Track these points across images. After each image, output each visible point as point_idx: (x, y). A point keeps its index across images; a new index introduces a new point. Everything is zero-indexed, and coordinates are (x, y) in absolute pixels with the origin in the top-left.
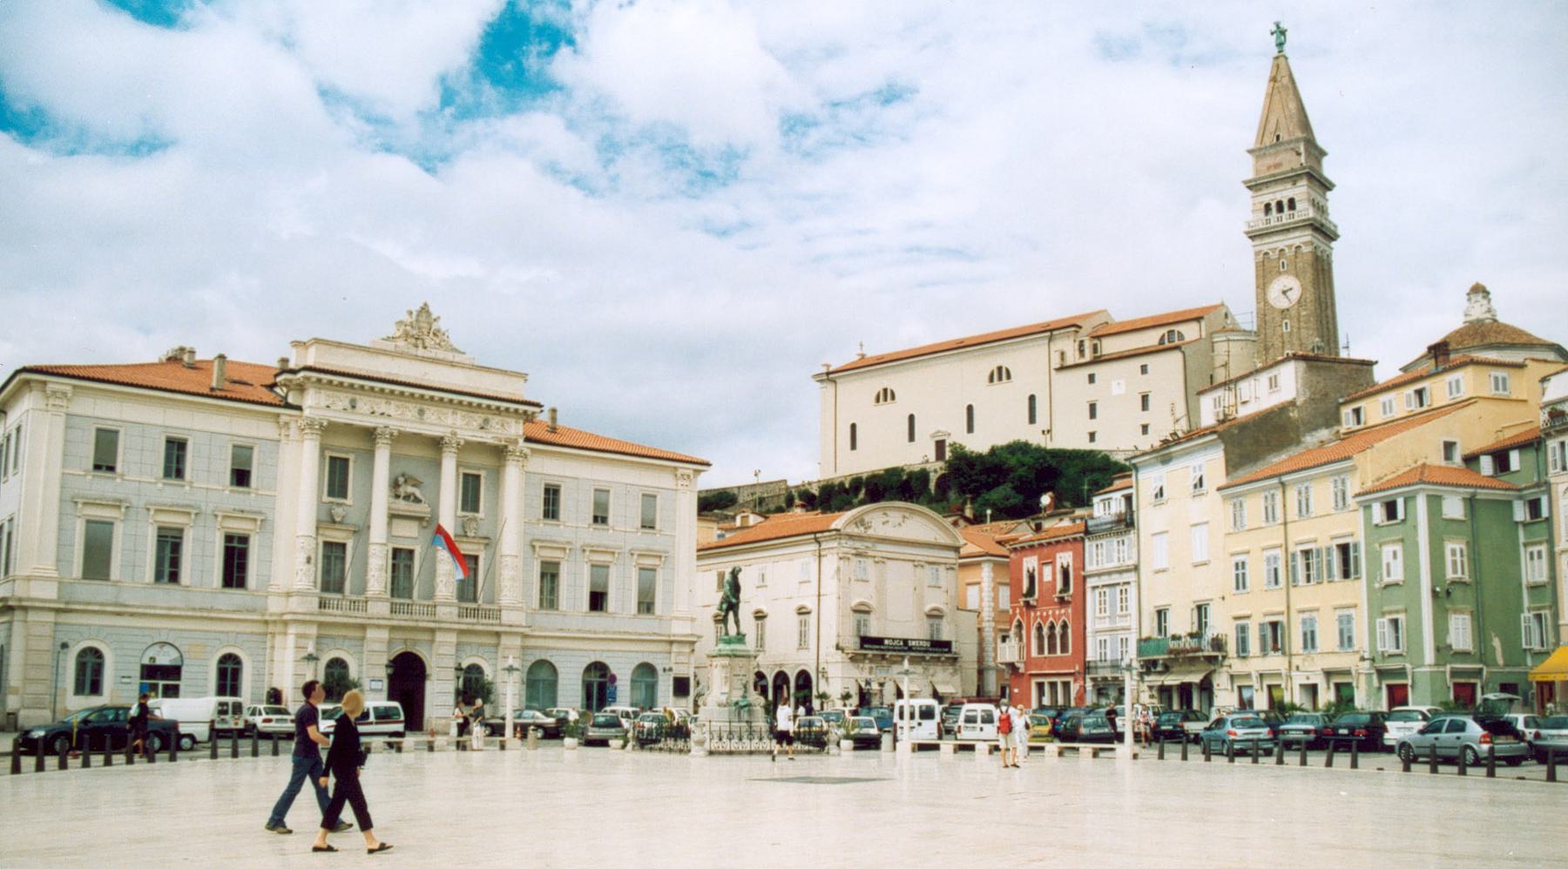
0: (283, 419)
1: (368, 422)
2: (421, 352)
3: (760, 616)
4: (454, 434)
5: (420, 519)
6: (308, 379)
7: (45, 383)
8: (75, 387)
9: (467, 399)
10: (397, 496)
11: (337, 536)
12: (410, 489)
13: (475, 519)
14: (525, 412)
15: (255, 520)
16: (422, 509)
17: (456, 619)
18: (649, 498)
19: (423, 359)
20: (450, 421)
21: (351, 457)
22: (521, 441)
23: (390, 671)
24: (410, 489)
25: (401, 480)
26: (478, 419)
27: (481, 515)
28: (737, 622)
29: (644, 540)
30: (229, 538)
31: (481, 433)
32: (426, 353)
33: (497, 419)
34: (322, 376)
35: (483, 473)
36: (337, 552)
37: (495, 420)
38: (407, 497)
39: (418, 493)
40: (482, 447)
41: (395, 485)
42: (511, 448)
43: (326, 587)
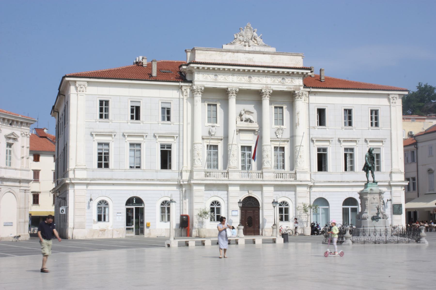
0: (183, 89)
1: (223, 86)
2: (247, 48)
3: (430, 171)
5: (253, 131)
6: (193, 67)
7: (75, 82)
8: (88, 82)
9: (272, 70)
10: (242, 120)
11: (213, 142)
13: (282, 129)
14: (303, 73)
15: (174, 137)
16: (255, 126)
17: (273, 179)
18: (375, 113)
19: (249, 52)
20: (264, 82)
22: (302, 88)
23: (241, 205)
25: (243, 112)
28: (373, 176)
29: (373, 133)
30: (162, 146)
32: (251, 49)
34: (199, 65)
38: (247, 120)
41: (241, 115)
42: (296, 92)
43: (209, 166)
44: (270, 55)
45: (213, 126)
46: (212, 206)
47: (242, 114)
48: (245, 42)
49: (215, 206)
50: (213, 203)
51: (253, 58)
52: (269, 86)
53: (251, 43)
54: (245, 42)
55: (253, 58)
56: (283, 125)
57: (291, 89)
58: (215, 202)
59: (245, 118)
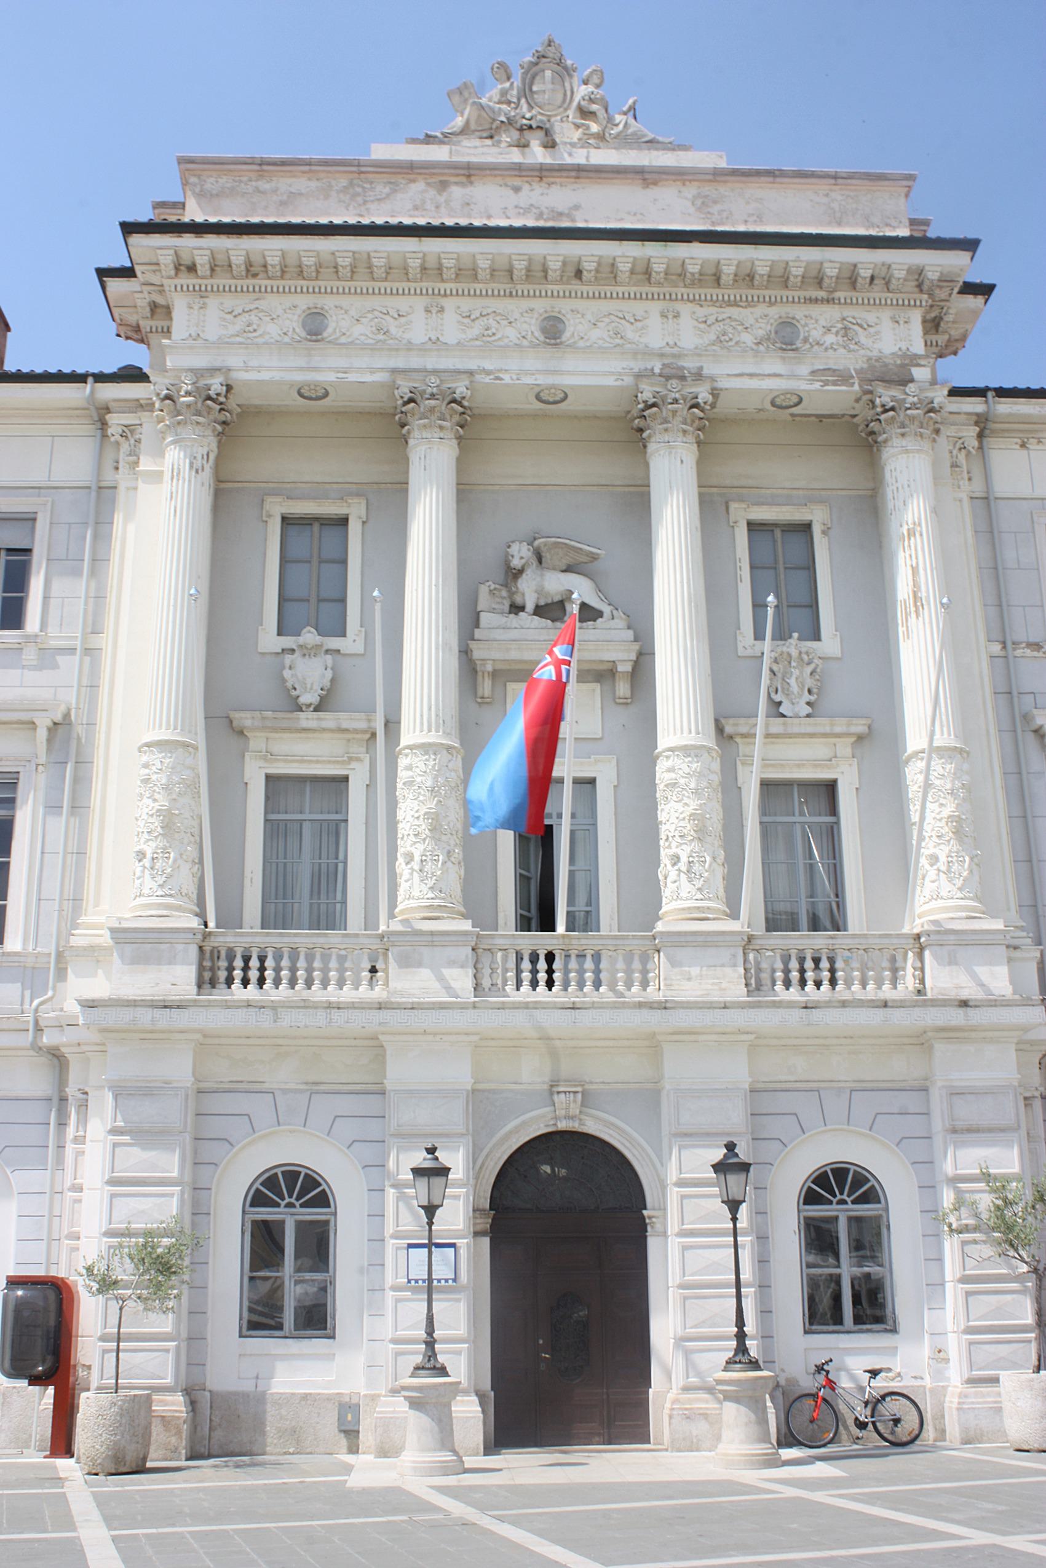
4: (673, 374)
10: (517, 608)
11: (307, 753)
12: (555, 583)
21: (355, 511)
24: (555, 583)
25: (520, 554)
26: (758, 320)
27: (830, 643)
31: (773, 364)
33: (828, 314)
35: (817, 516)
36: (309, 812)
37: (819, 321)
38: (551, 610)
39: (581, 590)
40: (791, 422)
44: (691, 190)
45: (308, 652)
46: (264, 1213)
47: (516, 563)
48: (521, 130)
49: (290, 1217)
50: (271, 1182)
51: (577, 207)
52: (690, 364)
53: (566, 132)
54: (521, 130)
55: (577, 207)
56: (817, 637)
57: (844, 378)
58: (292, 1176)
59: (540, 592)
